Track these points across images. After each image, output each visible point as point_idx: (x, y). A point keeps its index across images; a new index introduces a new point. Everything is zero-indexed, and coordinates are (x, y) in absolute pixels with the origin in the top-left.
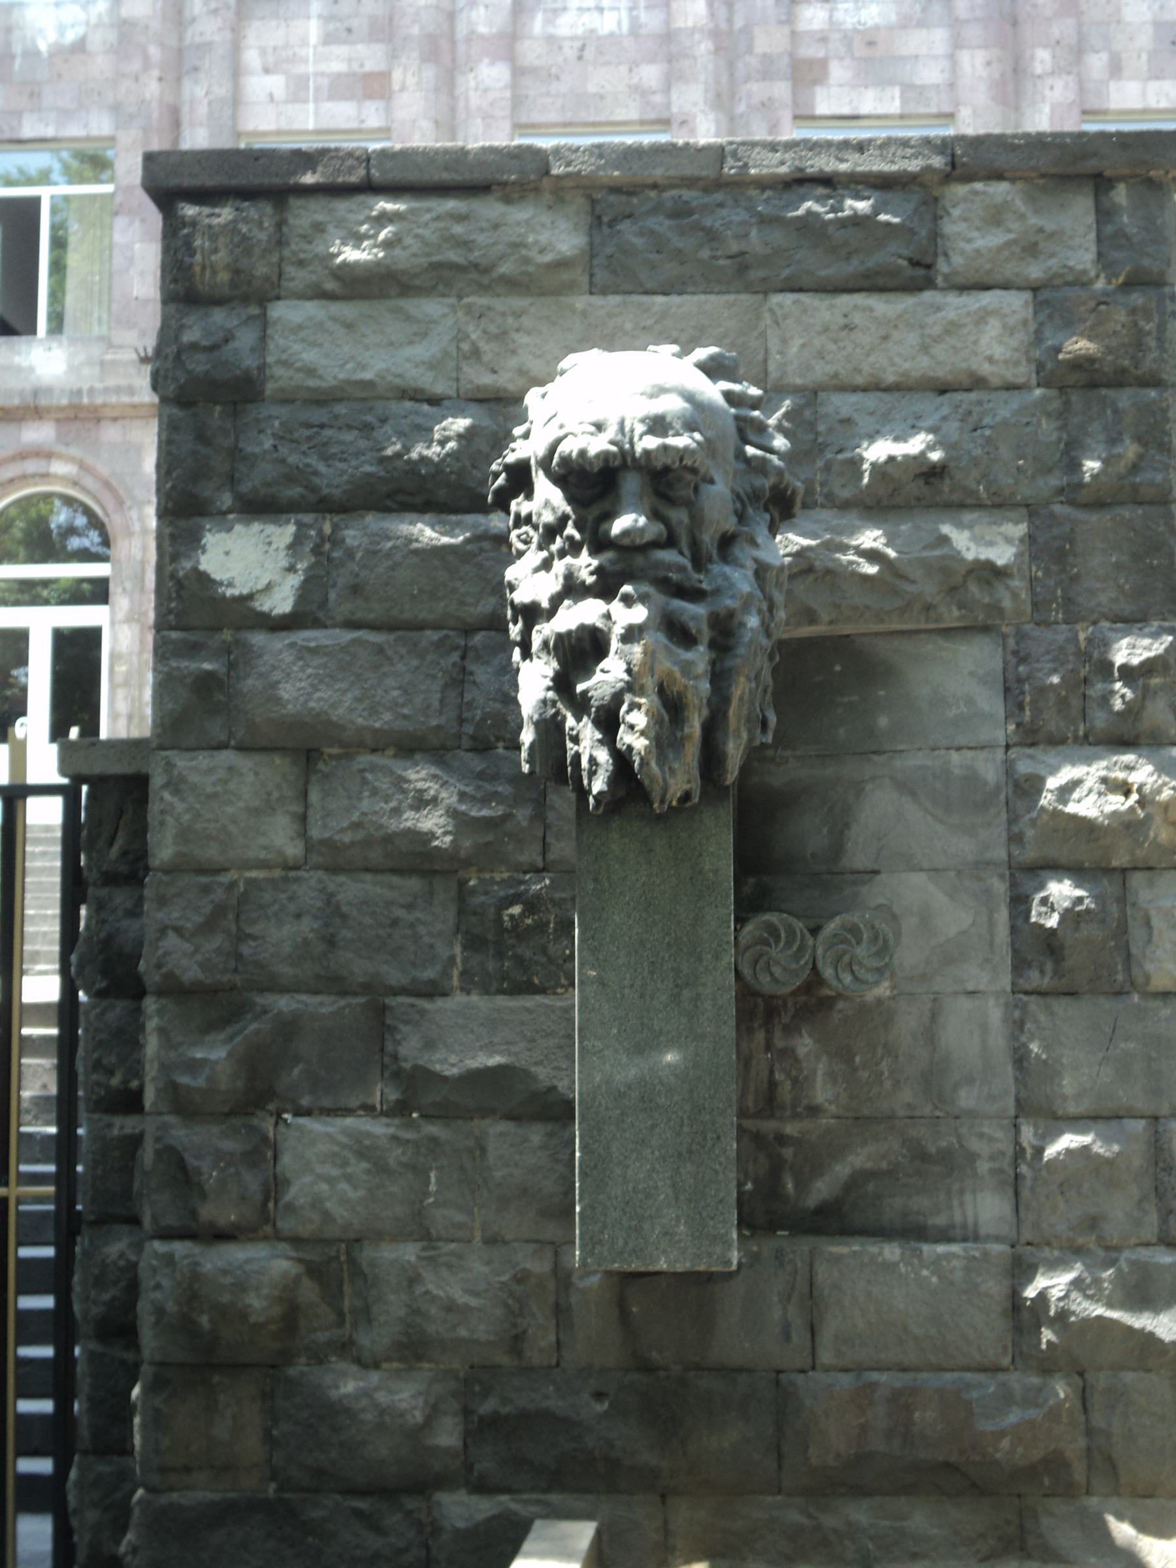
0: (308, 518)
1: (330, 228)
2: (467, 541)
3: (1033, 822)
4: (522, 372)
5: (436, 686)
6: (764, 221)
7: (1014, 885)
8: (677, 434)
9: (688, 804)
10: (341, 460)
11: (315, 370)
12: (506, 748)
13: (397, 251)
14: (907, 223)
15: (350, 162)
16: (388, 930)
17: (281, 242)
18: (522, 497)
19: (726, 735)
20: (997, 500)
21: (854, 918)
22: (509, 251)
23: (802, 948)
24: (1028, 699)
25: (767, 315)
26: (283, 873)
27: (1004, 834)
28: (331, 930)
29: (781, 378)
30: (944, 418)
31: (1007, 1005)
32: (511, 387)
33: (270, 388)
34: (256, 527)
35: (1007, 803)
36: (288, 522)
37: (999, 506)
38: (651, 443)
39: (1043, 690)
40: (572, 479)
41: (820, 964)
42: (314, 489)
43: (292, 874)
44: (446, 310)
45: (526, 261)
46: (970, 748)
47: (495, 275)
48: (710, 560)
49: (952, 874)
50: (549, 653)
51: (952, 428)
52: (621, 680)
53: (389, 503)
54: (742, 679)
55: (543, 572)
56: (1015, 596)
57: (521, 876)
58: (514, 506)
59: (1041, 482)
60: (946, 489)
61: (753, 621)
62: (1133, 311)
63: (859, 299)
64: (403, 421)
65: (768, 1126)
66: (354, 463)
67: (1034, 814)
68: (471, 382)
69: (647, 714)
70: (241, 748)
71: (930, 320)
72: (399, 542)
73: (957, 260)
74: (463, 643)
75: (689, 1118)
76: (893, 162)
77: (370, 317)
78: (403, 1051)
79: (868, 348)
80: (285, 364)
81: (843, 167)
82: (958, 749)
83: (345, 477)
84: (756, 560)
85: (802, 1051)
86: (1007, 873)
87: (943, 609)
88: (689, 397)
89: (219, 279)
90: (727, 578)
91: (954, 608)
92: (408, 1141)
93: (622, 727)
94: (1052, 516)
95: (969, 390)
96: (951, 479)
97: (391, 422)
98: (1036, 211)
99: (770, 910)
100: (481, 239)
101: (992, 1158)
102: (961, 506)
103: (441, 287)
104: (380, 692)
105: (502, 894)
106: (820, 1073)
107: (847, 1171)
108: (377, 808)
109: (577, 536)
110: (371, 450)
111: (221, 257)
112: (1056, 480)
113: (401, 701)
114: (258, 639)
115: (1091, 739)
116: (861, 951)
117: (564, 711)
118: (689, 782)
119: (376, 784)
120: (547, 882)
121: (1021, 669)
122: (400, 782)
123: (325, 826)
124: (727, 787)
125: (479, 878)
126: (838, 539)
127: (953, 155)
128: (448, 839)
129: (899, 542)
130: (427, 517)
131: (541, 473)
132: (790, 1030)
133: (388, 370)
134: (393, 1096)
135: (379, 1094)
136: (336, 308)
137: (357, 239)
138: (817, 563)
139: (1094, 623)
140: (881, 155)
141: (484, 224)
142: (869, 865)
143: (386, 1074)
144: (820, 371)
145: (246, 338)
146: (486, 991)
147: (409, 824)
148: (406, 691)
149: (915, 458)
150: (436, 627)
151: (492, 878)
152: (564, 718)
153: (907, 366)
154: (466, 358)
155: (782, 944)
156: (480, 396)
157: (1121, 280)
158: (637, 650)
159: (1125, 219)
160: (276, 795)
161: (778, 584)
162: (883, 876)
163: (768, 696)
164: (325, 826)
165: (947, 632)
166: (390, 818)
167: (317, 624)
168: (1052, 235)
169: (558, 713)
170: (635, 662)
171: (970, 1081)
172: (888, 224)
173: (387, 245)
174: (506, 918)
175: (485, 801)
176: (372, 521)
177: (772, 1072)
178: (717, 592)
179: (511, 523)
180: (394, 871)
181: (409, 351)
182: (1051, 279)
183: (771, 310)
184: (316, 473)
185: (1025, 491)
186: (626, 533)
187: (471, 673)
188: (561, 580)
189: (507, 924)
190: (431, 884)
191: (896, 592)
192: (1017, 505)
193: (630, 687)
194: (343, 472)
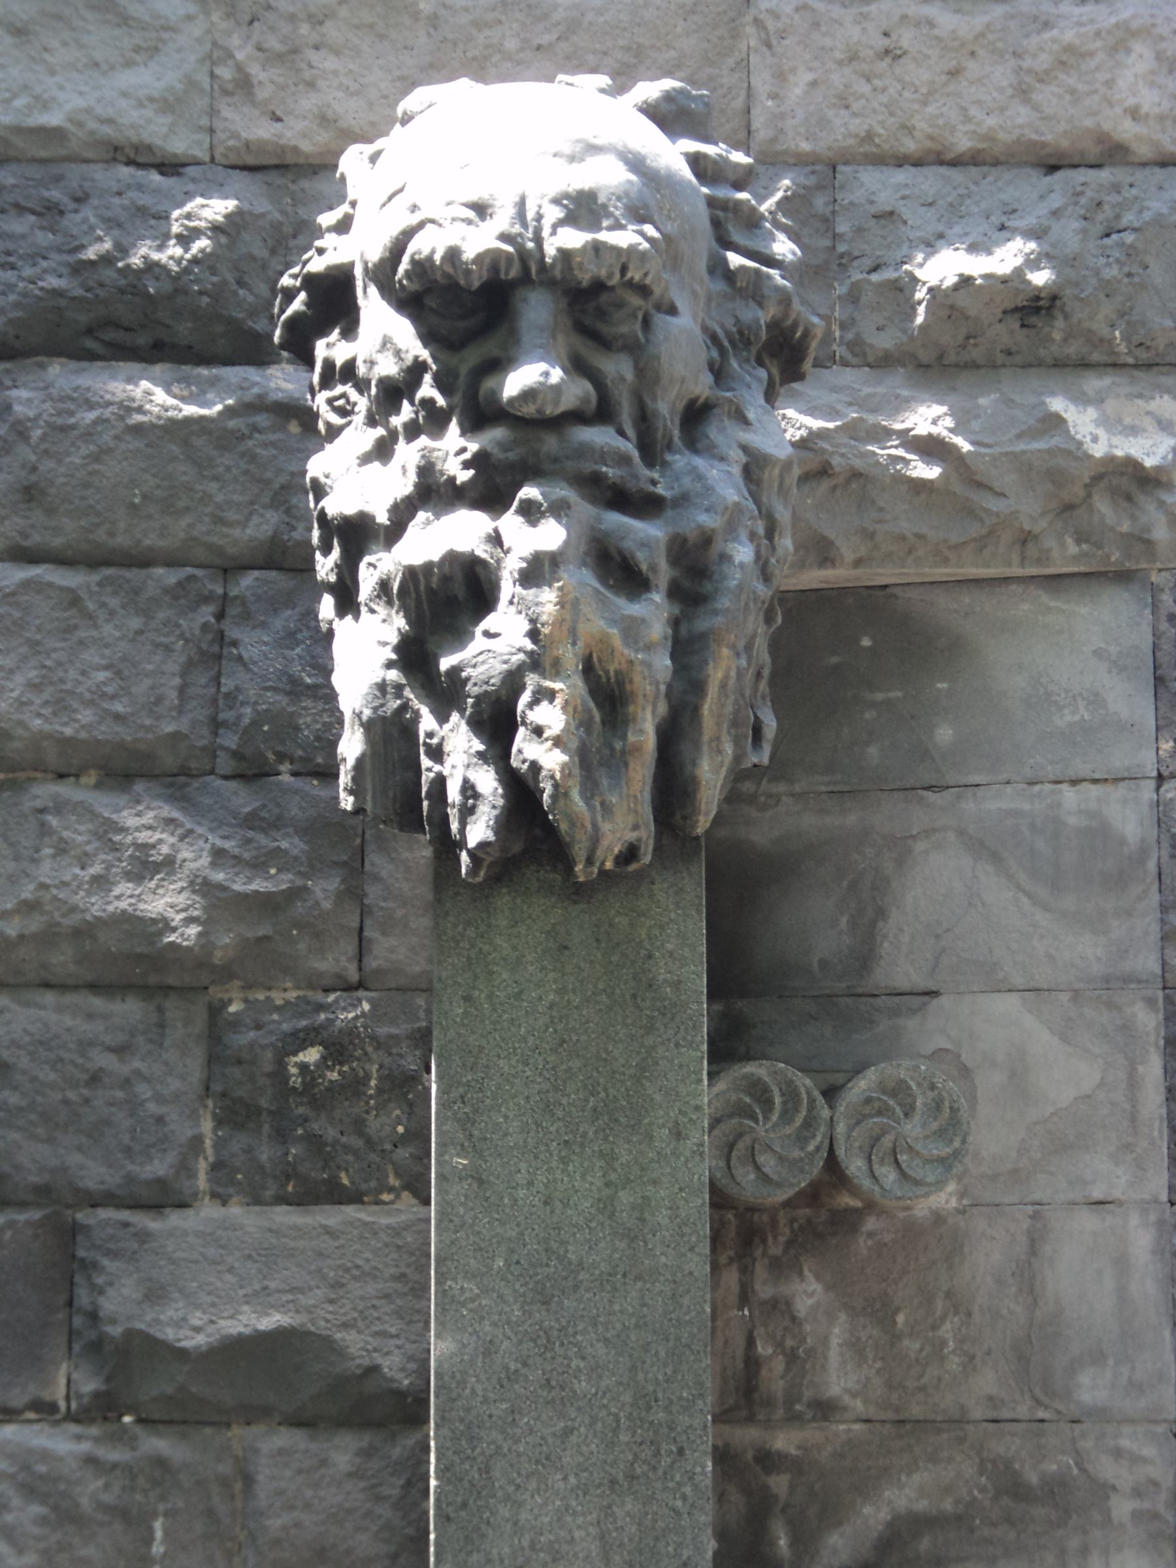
2: (228, 412)
4: (324, 120)
5: (173, 666)
8: (617, 226)
9: (633, 867)
12: (295, 774)
16: (85, 1092)
18: (336, 332)
19: (697, 745)
20: (1144, 355)
21: (901, 1070)
25: (750, 30)
27: (1155, 928)
29: (774, 140)
30: (1055, 213)
31: (1160, 1223)
32: (306, 146)
35: (1160, 874)
37: (1149, 366)
38: (573, 239)
40: (431, 302)
41: (841, 1152)
46: (1095, 781)
48: (669, 447)
49: (1064, 997)
50: (390, 603)
51: (1069, 232)
52: (520, 650)
53: (90, 344)
54: (725, 651)
55: (376, 465)
57: (319, 997)
58: (320, 350)
60: (1057, 336)
61: (743, 553)
64: (116, 201)
65: (746, 1436)
66: (28, 272)
68: (235, 135)
71: (1032, 43)
72: (107, 413)
74: (220, 591)
75: (629, 1417)
77: (59, 17)
78: (108, 1305)
79: (924, 90)
82: (1074, 782)
83: (12, 298)
84: (745, 449)
85: (802, 1306)
86: (1160, 994)
87: (1050, 542)
88: (636, 163)
90: (699, 477)
91: (1069, 541)
92: (115, 1466)
93: (521, 732)
95: (1098, 166)
96: (1066, 317)
97: (94, 202)
99: (748, 1057)
101: (1137, 1493)
102: (1084, 365)
104: (72, 674)
105: (285, 1027)
106: (835, 1341)
107: (884, 1515)
108: (67, 878)
109: (441, 401)
110: (60, 250)
113: (109, 689)
116: (912, 1129)
117: (416, 704)
118: (636, 827)
119: (66, 834)
120: (366, 1006)
122: (107, 832)
124: (697, 838)
125: (246, 1001)
126: (871, 419)
128: (193, 930)
129: (975, 425)
130: (158, 369)
131: (373, 290)
132: (780, 1268)
133: (88, 111)
134: (89, 1385)
135: (63, 1381)
138: (836, 461)
142: (923, 984)
143: (77, 1348)
146: (256, 1200)
147: (123, 905)
148: (119, 673)
149: (1005, 280)
150: (171, 562)
152: (417, 715)
153: (991, 121)
154: (226, 93)
156: (250, 160)
158: (547, 599)
161: (783, 491)
162: (944, 1001)
163: (763, 685)
165: (1055, 582)
166: (89, 893)
169: (405, 707)
170: (544, 618)
171: (1097, 1357)
174: (294, 1070)
175: (258, 866)
177: (750, 1342)
178: (682, 500)
179: (316, 379)
180: (94, 987)
181: (127, 79)
183: (757, 22)
186: (528, 395)
187: (235, 644)
188: (412, 477)
189: (296, 1081)
190: (160, 1010)
191: (970, 512)
193: (535, 663)
194: (11, 287)
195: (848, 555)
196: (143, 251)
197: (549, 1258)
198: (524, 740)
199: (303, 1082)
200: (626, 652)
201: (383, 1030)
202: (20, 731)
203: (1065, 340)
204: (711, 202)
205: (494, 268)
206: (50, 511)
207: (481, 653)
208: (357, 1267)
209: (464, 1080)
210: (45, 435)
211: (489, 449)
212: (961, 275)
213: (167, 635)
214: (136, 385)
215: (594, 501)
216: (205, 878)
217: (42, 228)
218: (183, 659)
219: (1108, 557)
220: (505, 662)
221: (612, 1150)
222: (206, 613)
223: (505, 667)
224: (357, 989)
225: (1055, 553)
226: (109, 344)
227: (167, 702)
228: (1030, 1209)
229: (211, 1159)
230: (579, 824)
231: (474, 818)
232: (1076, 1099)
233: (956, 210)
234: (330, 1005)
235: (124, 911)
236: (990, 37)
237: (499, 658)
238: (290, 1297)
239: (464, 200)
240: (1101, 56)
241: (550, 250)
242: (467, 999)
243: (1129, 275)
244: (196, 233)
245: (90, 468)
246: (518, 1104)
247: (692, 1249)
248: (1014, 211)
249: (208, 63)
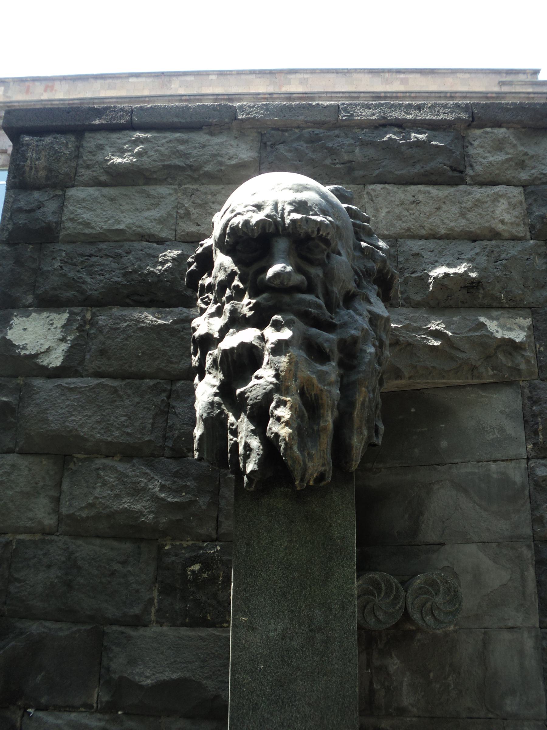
0: (76, 310)
1: (107, 148)
2: (174, 322)
6: (364, 144)
7: (537, 552)
8: (316, 214)
9: (323, 483)
10: (100, 275)
11: (89, 223)
13: (145, 158)
14: (448, 146)
15: (121, 113)
16: (108, 579)
17: (78, 157)
22: (210, 159)
23: (397, 597)
25: (366, 196)
26: (42, 537)
27: (529, 517)
28: (70, 577)
33: (63, 233)
34: (45, 314)
35: (530, 496)
36: (64, 312)
37: (514, 308)
40: (239, 247)
41: (410, 610)
42: (82, 292)
43: (48, 537)
44: (171, 192)
45: (221, 163)
46: (503, 461)
47: (201, 172)
48: (338, 306)
49: (494, 545)
50: (217, 369)
51: (482, 260)
52: (271, 383)
53: (128, 301)
55: (217, 318)
56: (528, 362)
57: (200, 544)
59: (538, 294)
63: (421, 187)
64: (141, 252)
66: (108, 276)
68: (183, 231)
69: (291, 409)
70: (23, 453)
71: (465, 199)
72: (131, 324)
73: (478, 168)
74: (169, 388)
76: (438, 115)
77: (126, 195)
78: (114, 666)
79: (428, 214)
80: (72, 220)
81: (409, 117)
82: (495, 461)
83: (102, 285)
84: (370, 312)
85: (392, 669)
86: (532, 543)
89: (39, 175)
91: (489, 369)
95: (491, 240)
96: (484, 289)
97: (133, 253)
98: (522, 145)
100: (194, 152)
102: (490, 307)
103: (169, 180)
104: (112, 418)
106: (405, 684)
108: (105, 495)
109: (241, 286)
110: (120, 269)
111: (42, 163)
113: (126, 424)
114: (38, 382)
117: (226, 411)
119: (106, 478)
120: (219, 548)
121: (534, 408)
123: (71, 505)
124: (352, 473)
125: (172, 545)
127: (473, 113)
128: (151, 516)
130: (151, 309)
131: (218, 251)
133: (133, 224)
135: (96, 696)
137: (121, 152)
138: (401, 339)
140: (431, 112)
141: (197, 145)
143: (102, 682)
144: (399, 227)
145: (51, 207)
146: (174, 624)
147: (126, 506)
148: (129, 418)
149: (461, 275)
151: (181, 545)
152: (227, 417)
153: (452, 224)
154: (181, 218)
155: (382, 595)
156: (188, 239)
158: (283, 361)
160: (41, 484)
162: (447, 547)
164: (71, 505)
165: (484, 386)
167: (77, 374)
168: (532, 157)
169: (222, 412)
170: (282, 369)
172: (437, 146)
174: (189, 573)
175: (177, 491)
176: (116, 311)
177: (371, 683)
178: (344, 325)
180: (114, 538)
181: (147, 214)
182: (534, 180)
183: (368, 193)
184: (84, 282)
185: (529, 299)
186: (277, 275)
187: (174, 407)
189: (190, 577)
191: (452, 358)
192: (524, 308)
193: (278, 388)
195: (407, 374)
196: (148, 268)
197: (284, 665)
198: (272, 423)
199: (193, 578)
200: (320, 386)
201: (225, 558)
202: (91, 439)
203: (483, 298)
204: (354, 224)
205: (264, 228)
206: (109, 359)
207: (254, 385)
208: (213, 653)
209: (246, 581)
210: (109, 331)
211: (260, 301)
212: (445, 273)
213: (148, 404)
214: (143, 314)
215: (306, 324)
216: (157, 496)
217: (114, 262)
218: (154, 413)
219: (504, 375)
220: (264, 389)
221: (313, 614)
222: (164, 396)
223: (264, 391)
224: (216, 541)
226: (134, 301)
227: (147, 429)
228: (483, 630)
229: (157, 608)
230: (297, 462)
231: (249, 460)
232: (500, 586)
233: (441, 254)
234: (204, 547)
235: (126, 508)
236: (450, 197)
237: (262, 388)
238: (185, 665)
239: (252, 204)
240: (489, 203)
241: (287, 221)
242: (248, 544)
243: (505, 275)
244: (167, 261)
245: (124, 343)
246: (270, 593)
247: (350, 661)
248: (462, 254)
249: (176, 209)
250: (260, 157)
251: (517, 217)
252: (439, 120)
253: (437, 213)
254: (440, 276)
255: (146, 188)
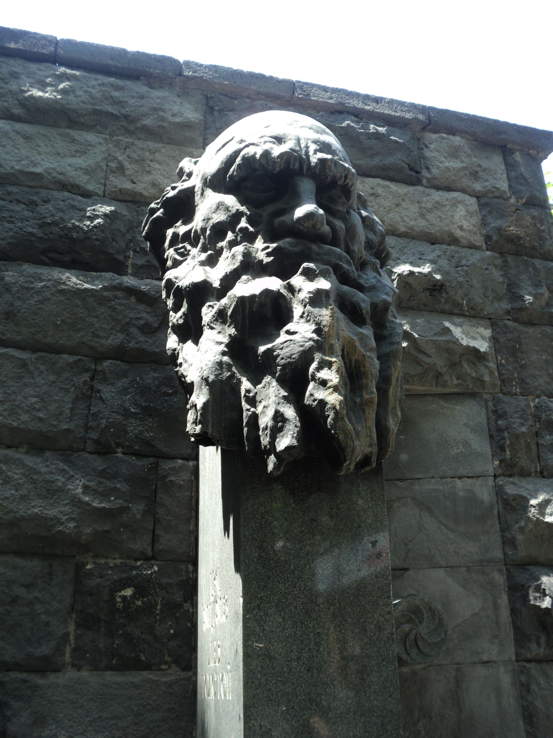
2: (105, 288)
3: (522, 529)
5: (67, 399)
7: (510, 577)
9: (368, 469)
10: (8, 222)
12: (124, 453)
13: (71, 97)
14: (407, 144)
16: (8, 608)
22: (150, 112)
24: (508, 442)
27: (499, 539)
32: (145, 193)
35: (499, 516)
37: (474, 317)
39: (517, 437)
44: (101, 141)
45: (163, 119)
46: (468, 477)
47: (139, 125)
49: (463, 570)
51: (444, 262)
52: (310, 339)
53: (43, 258)
57: (133, 563)
59: (496, 305)
62: (533, 218)
63: (378, 181)
64: (62, 203)
66: (19, 224)
67: (522, 523)
68: (115, 187)
69: (337, 371)
72: (49, 284)
73: (435, 171)
74: (93, 367)
76: (396, 112)
79: (388, 208)
81: (367, 108)
82: (460, 478)
83: (11, 234)
86: (504, 567)
91: (454, 378)
93: (311, 385)
94: (505, 326)
100: (132, 101)
103: (98, 127)
104: (19, 397)
108: (8, 495)
110: (34, 219)
112: (505, 305)
115: (545, 474)
117: (238, 375)
119: (9, 473)
120: (156, 568)
121: (500, 422)
125: (95, 563)
128: (72, 525)
130: (73, 271)
133: (54, 169)
136: (18, 126)
137: (43, 86)
139: (538, 397)
140: (389, 107)
141: (135, 94)
146: (96, 668)
147: (36, 510)
148: (42, 400)
149: (425, 275)
152: (239, 382)
153: (412, 223)
154: (112, 172)
156: (120, 197)
157: (524, 200)
159: (522, 169)
162: (411, 572)
165: (446, 396)
169: (233, 376)
170: (324, 323)
172: (396, 142)
173: (64, 92)
174: (119, 600)
175: (105, 495)
176: (28, 269)
180: (16, 553)
181: (71, 160)
182: (487, 193)
185: (489, 309)
187: (99, 391)
189: (120, 605)
191: (418, 363)
192: (483, 318)
194: (10, 229)
196: (73, 221)
197: (311, 704)
198: (314, 388)
199: (123, 606)
200: (362, 350)
201: (164, 581)
203: (445, 303)
205: (288, 163)
207: (286, 342)
208: (149, 704)
209: (259, 596)
210: (19, 290)
211: (283, 246)
212: (410, 271)
213: (67, 385)
214: (64, 275)
216: (79, 499)
217: (27, 210)
218: (74, 396)
219: (468, 386)
220: (301, 346)
221: (344, 637)
222: (86, 377)
223: (301, 349)
224: (150, 560)
225: (449, 383)
227: (64, 415)
228: (455, 666)
229: (73, 646)
230: (350, 436)
231: (282, 434)
232: (472, 615)
234: (138, 567)
235: (36, 513)
236: (409, 195)
237: (298, 344)
238: (114, 722)
239: (270, 135)
240: (448, 207)
243: (467, 281)
244: (97, 217)
245: (38, 306)
246: (290, 611)
247: (391, 696)
248: (424, 254)
249: (106, 161)
250: (205, 121)
251: (474, 226)
252: (397, 117)
253: (397, 210)
254: (405, 273)
255: (70, 131)
